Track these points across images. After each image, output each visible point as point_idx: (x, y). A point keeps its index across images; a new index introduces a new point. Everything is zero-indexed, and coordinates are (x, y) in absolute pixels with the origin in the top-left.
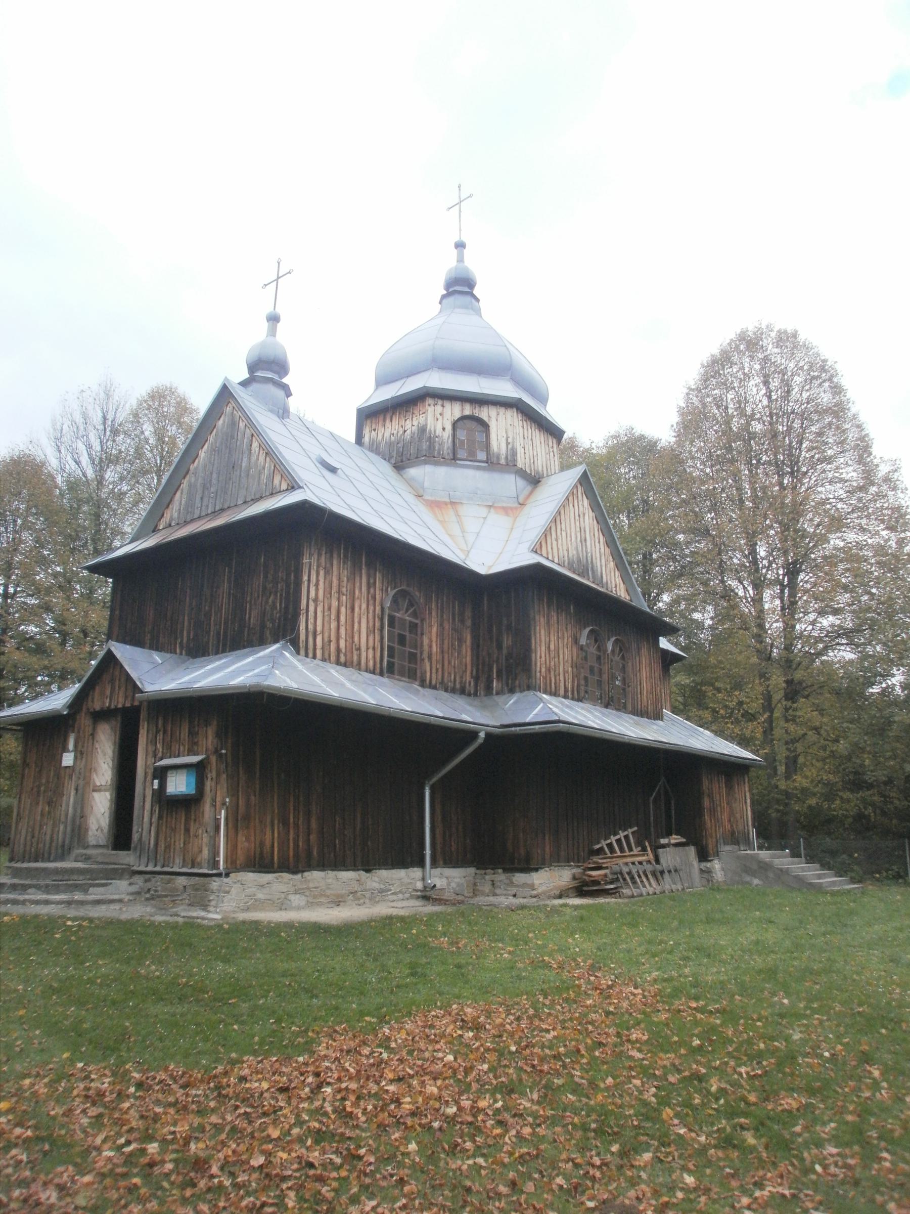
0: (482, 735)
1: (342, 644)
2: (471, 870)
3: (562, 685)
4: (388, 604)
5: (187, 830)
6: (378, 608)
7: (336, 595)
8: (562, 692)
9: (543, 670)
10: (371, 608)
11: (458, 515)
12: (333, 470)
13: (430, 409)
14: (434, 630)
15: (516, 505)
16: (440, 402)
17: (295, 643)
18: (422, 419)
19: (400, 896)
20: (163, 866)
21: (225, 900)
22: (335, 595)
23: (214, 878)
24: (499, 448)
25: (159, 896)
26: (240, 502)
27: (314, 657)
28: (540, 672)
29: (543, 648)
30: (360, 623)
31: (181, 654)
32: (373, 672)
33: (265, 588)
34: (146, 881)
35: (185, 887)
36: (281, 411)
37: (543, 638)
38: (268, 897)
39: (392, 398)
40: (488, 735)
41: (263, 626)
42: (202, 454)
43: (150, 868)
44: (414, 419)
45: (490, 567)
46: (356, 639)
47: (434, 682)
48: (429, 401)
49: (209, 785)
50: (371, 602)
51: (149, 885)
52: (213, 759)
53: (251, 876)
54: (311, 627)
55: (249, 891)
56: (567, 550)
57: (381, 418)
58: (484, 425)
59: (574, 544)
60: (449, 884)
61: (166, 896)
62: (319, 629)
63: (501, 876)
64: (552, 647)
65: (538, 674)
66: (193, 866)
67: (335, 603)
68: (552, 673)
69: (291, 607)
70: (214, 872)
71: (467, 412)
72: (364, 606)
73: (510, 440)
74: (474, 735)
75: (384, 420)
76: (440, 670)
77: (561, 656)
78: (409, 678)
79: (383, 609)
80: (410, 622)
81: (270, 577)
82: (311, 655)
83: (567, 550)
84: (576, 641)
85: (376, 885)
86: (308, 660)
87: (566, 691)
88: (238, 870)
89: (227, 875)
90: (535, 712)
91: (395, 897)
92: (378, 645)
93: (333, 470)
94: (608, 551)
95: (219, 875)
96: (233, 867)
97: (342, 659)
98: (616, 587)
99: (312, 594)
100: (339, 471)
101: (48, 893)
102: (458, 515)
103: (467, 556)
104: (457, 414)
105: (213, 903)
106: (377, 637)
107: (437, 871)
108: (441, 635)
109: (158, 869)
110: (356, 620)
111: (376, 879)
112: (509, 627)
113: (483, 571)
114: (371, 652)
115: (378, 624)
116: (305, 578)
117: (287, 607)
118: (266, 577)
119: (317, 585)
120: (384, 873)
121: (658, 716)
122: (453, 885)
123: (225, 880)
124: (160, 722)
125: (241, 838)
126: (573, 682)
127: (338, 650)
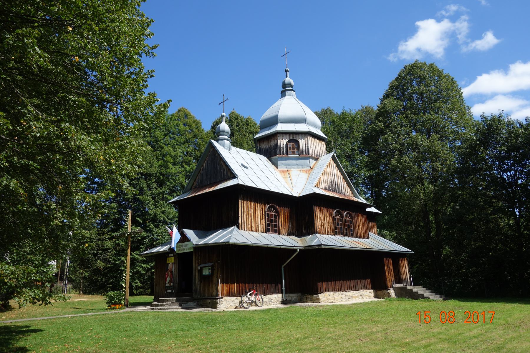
1: (253, 225)
2: (299, 294)
3: (327, 230)
4: (266, 210)
5: (209, 286)
6: (264, 212)
7: (250, 210)
8: (327, 233)
9: (319, 226)
10: (261, 212)
11: (289, 175)
12: (247, 168)
14: (282, 216)
15: (310, 169)
16: (282, 135)
17: (238, 227)
19: (276, 303)
20: (202, 297)
21: (222, 305)
22: (249, 210)
23: (218, 299)
24: (303, 149)
26: (218, 181)
27: (244, 230)
28: (318, 227)
29: (319, 219)
30: (258, 217)
32: (263, 232)
34: (198, 302)
36: (229, 148)
37: (318, 216)
38: (234, 304)
40: (300, 250)
44: (274, 141)
45: (300, 194)
46: (257, 223)
47: (283, 233)
48: (279, 135)
49: (215, 272)
50: (261, 210)
52: (216, 264)
53: (228, 298)
54: (243, 221)
55: (228, 303)
56: (328, 183)
59: (330, 181)
60: (292, 299)
61: (204, 306)
62: (245, 221)
63: (309, 296)
64: (322, 218)
65: (317, 228)
66: (212, 296)
67: (250, 212)
68: (323, 227)
71: (291, 138)
72: (259, 212)
73: (307, 145)
74: (296, 250)
75: (264, 142)
76: (285, 229)
77: (326, 221)
78: (275, 232)
79: (265, 212)
80: (274, 215)
82: (243, 229)
83: (328, 183)
84: (331, 214)
85: (268, 300)
86: (243, 231)
87: (328, 232)
88: (225, 297)
89: (222, 298)
90: (315, 242)
91: (273, 304)
92: (264, 223)
93: (247, 168)
94: (344, 180)
95: (220, 298)
96: (223, 295)
97: (253, 229)
98: (348, 193)
99: (242, 211)
100: (249, 168)
101: (171, 306)
102: (289, 175)
103: (292, 190)
105: (218, 307)
106: (264, 221)
107: (287, 295)
108: (285, 218)
109: (201, 298)
110: (257, 217)
111: (267, 298)
113: (297, 195)
114: (262, 225)
115: (264, 217)
116: (240, 206)
119: (244, 208)
120: (270, 296)
121: (367, 237)
122: (293, 299)
123: (222, 300)
124: (199, 253)
125: (225, 288)
126: (331, 229)
127: (251, 227)
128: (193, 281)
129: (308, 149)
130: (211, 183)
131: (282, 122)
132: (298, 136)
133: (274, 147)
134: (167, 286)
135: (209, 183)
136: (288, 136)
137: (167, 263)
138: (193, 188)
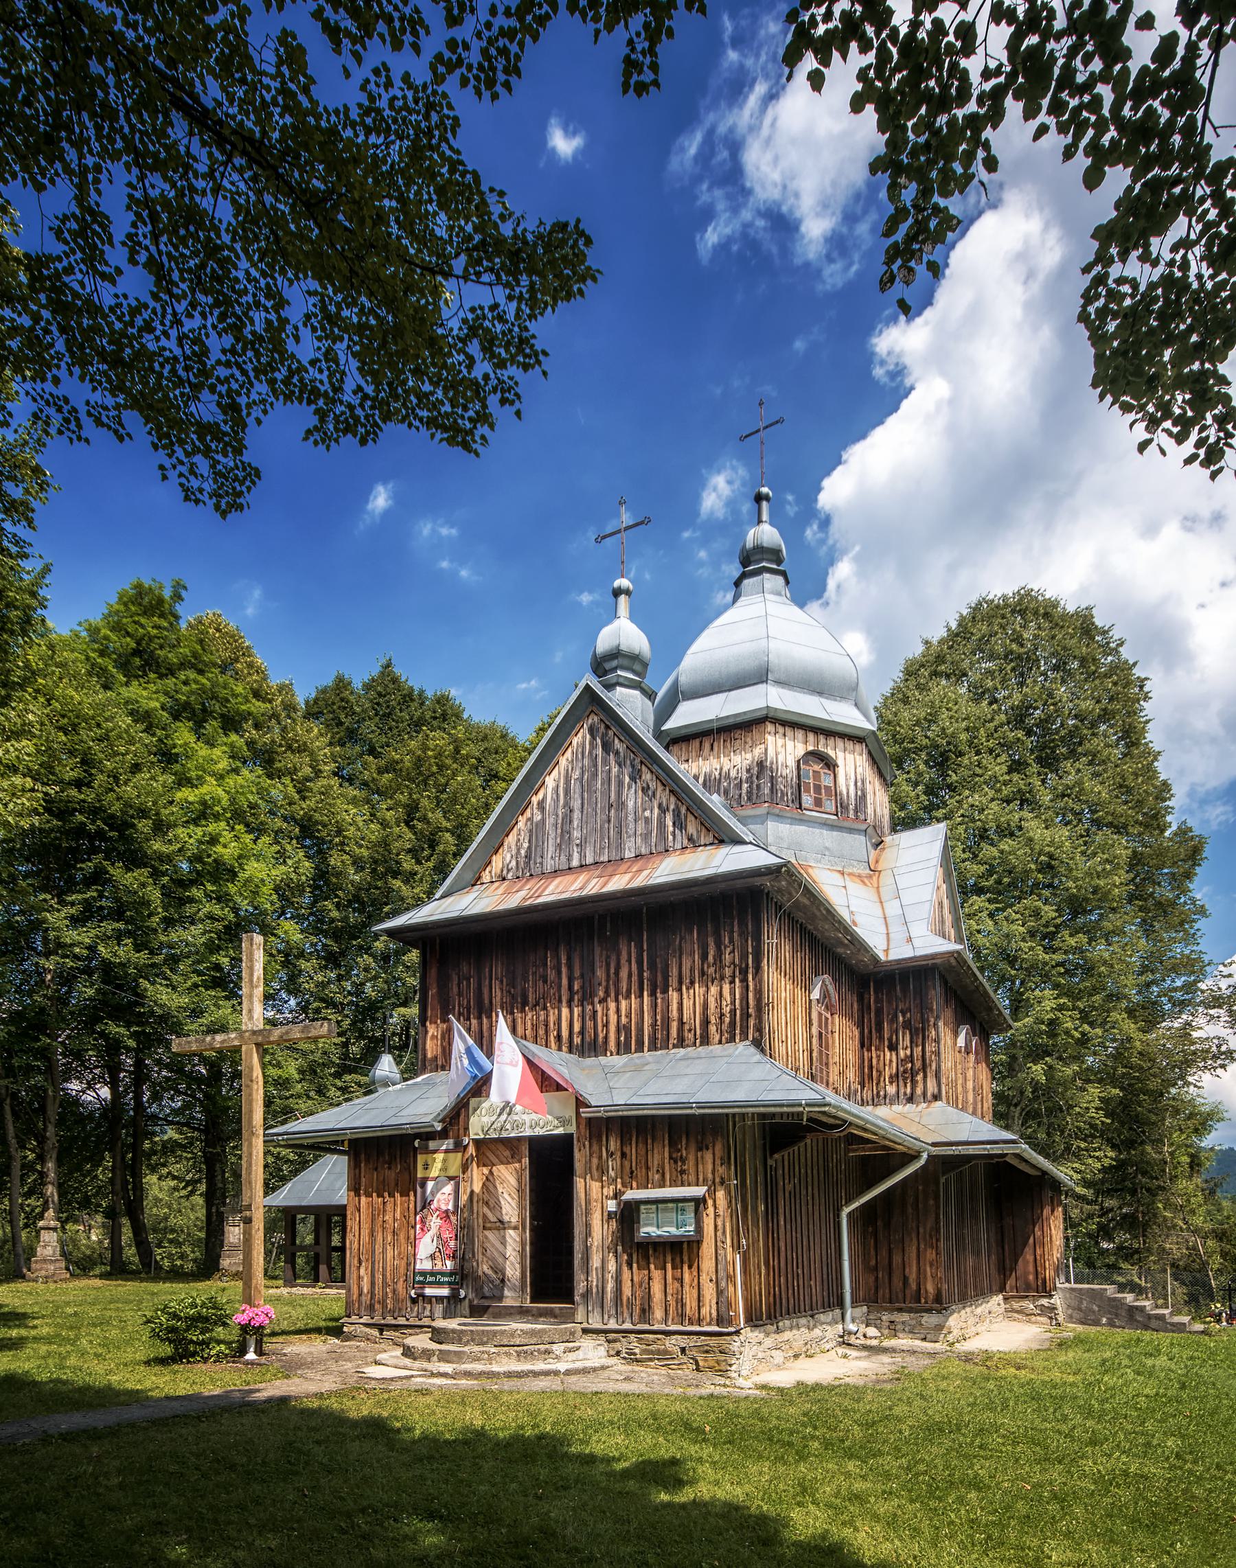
0: (925, 1155)
13: (770, 739)
16: (781, 729)
18: (758, 751)
25: (637, 1361)
31: (560, 1049)
33: (703, 973)
35: (683, 1350)
39: (718, 719)
41: (706, 1022)
42: (550, 781)
43: (612, 1325)
48: (770, 727)
51: (617, 1346)
57: (697, 742)
58: (830, 765)
69: (751, 995)
70: (731, 1329)
71: (811, 748)
81: (711, 958)
104: (801, 750)
109: (628, 1326)
112: (907, 1025)
117: (745, 998)
118: (704, 957)
128: (578, 1257)
129: (864, 796)
130: (589, 860)
131: (778, 683)
132: (831, 741)
133: (748, 771)
134: (423, 1273)
135: (575, 863)
136: (800, 734)
137: (419, 1175)
138: (486, 877)
